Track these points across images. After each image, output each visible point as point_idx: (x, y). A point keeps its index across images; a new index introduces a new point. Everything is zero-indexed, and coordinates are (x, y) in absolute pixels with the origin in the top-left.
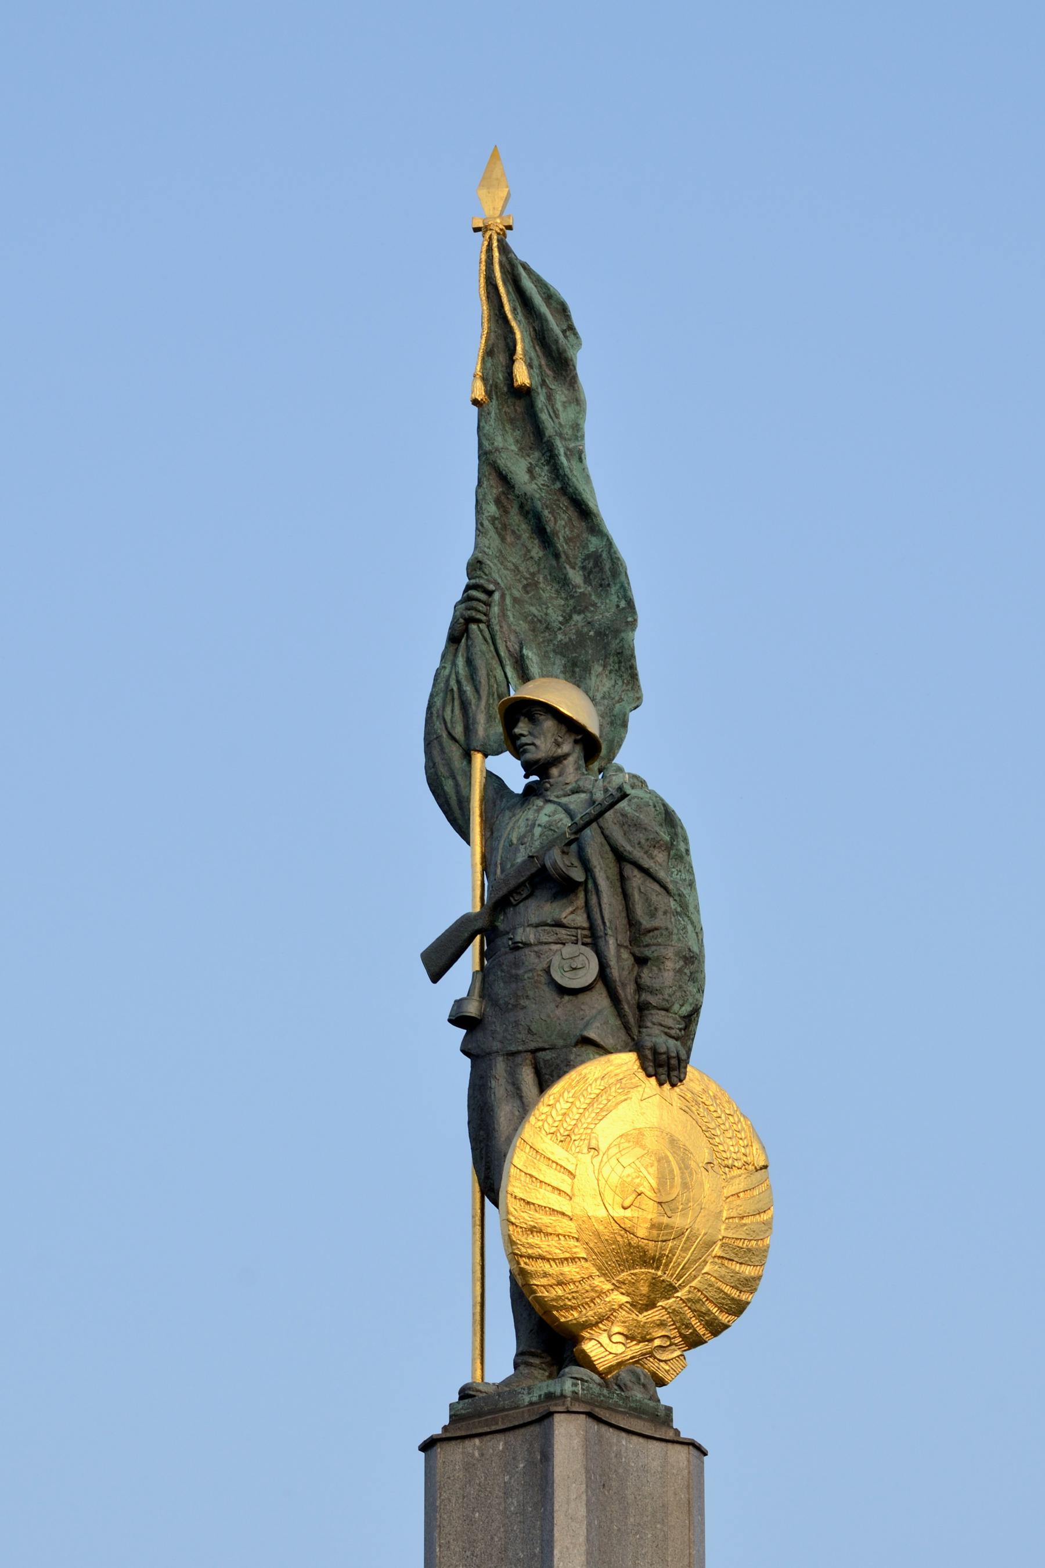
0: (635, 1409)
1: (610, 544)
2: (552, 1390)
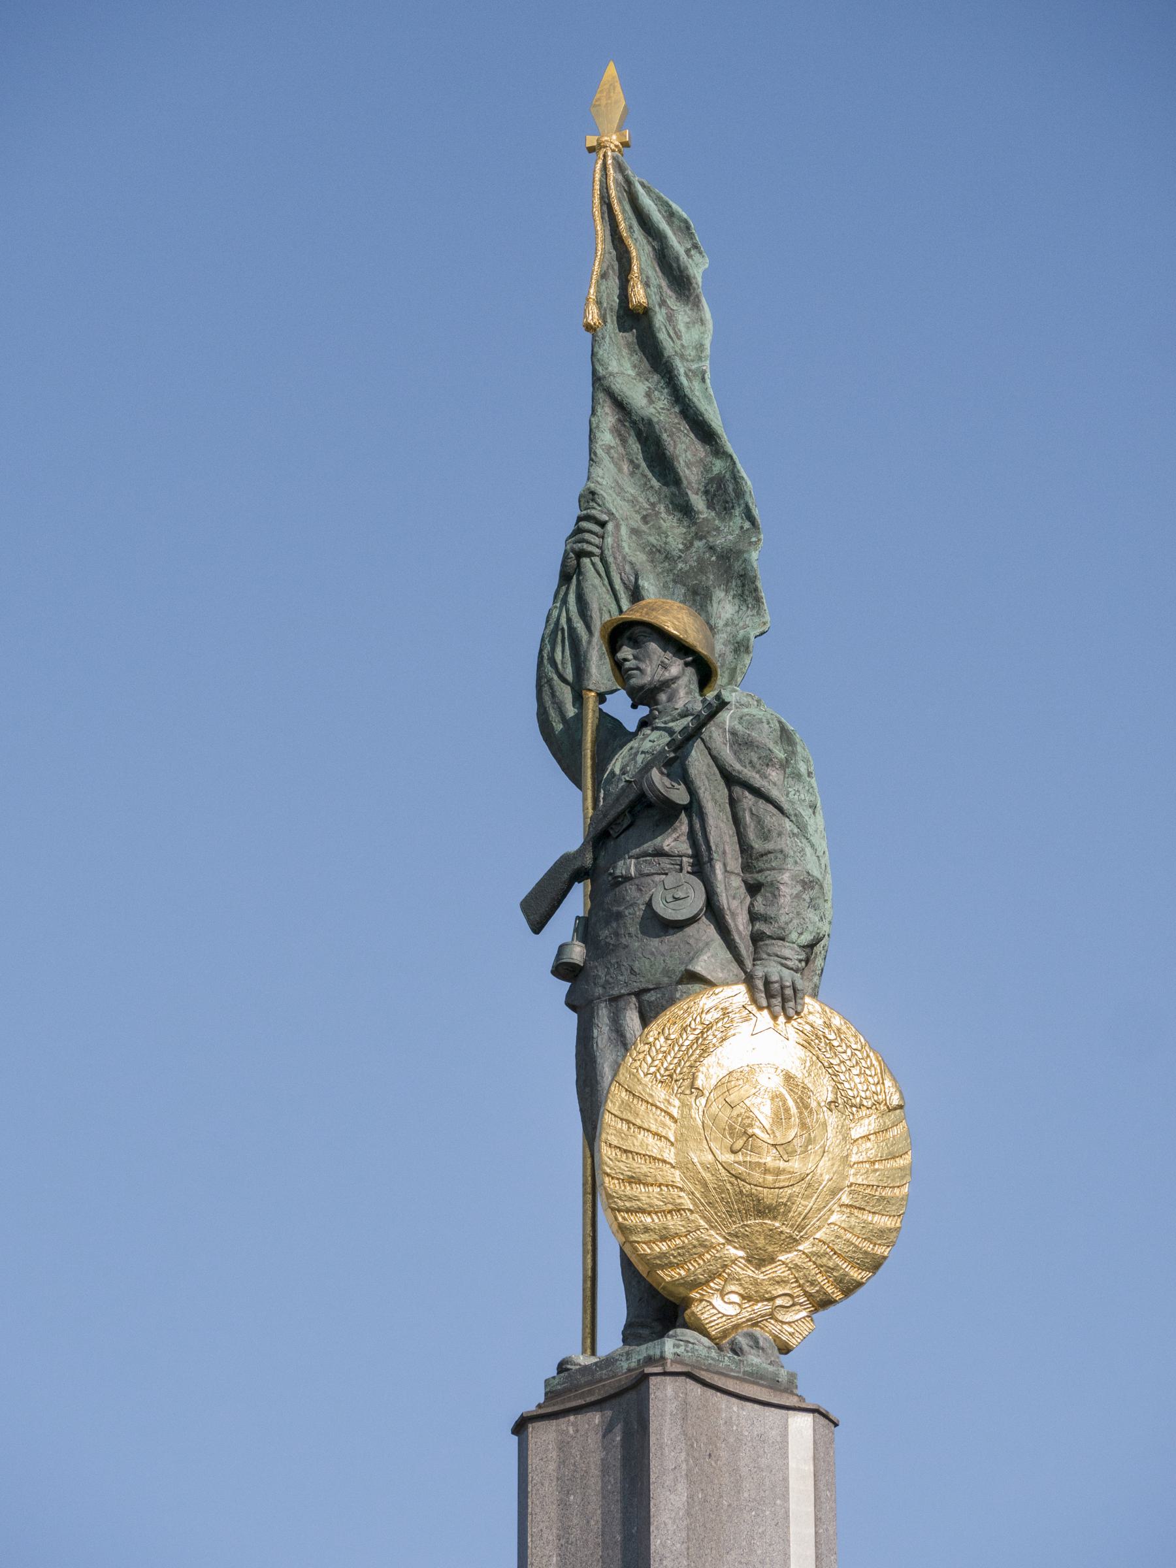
0: (751, 1374)
2: (651, 1353)
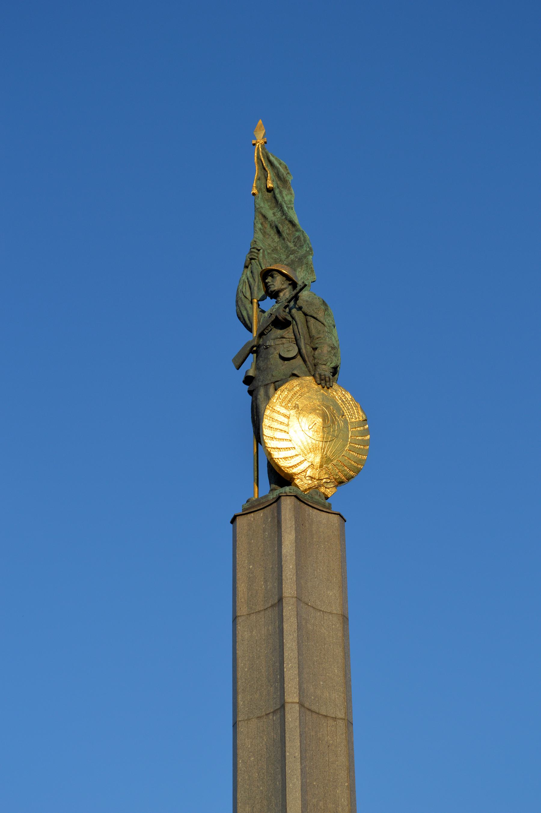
0: (316, 502)
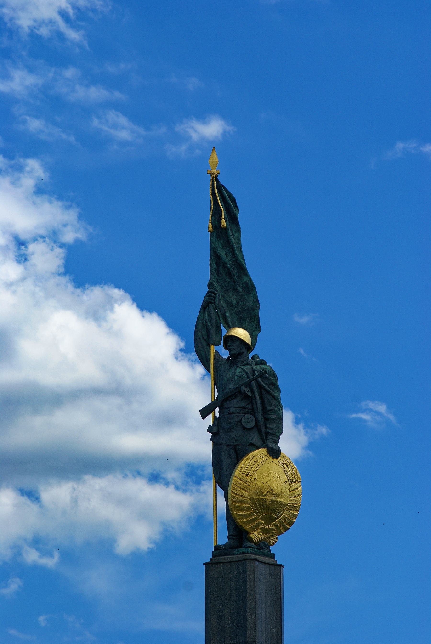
1: (251, 280)
2: (244, 551)
